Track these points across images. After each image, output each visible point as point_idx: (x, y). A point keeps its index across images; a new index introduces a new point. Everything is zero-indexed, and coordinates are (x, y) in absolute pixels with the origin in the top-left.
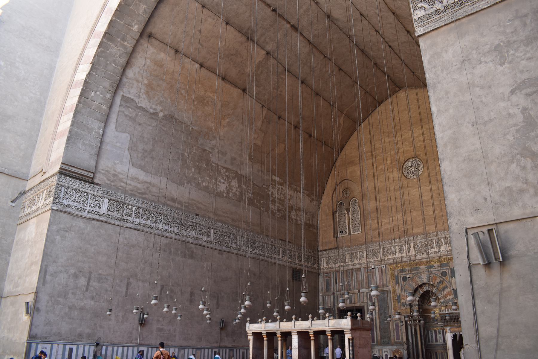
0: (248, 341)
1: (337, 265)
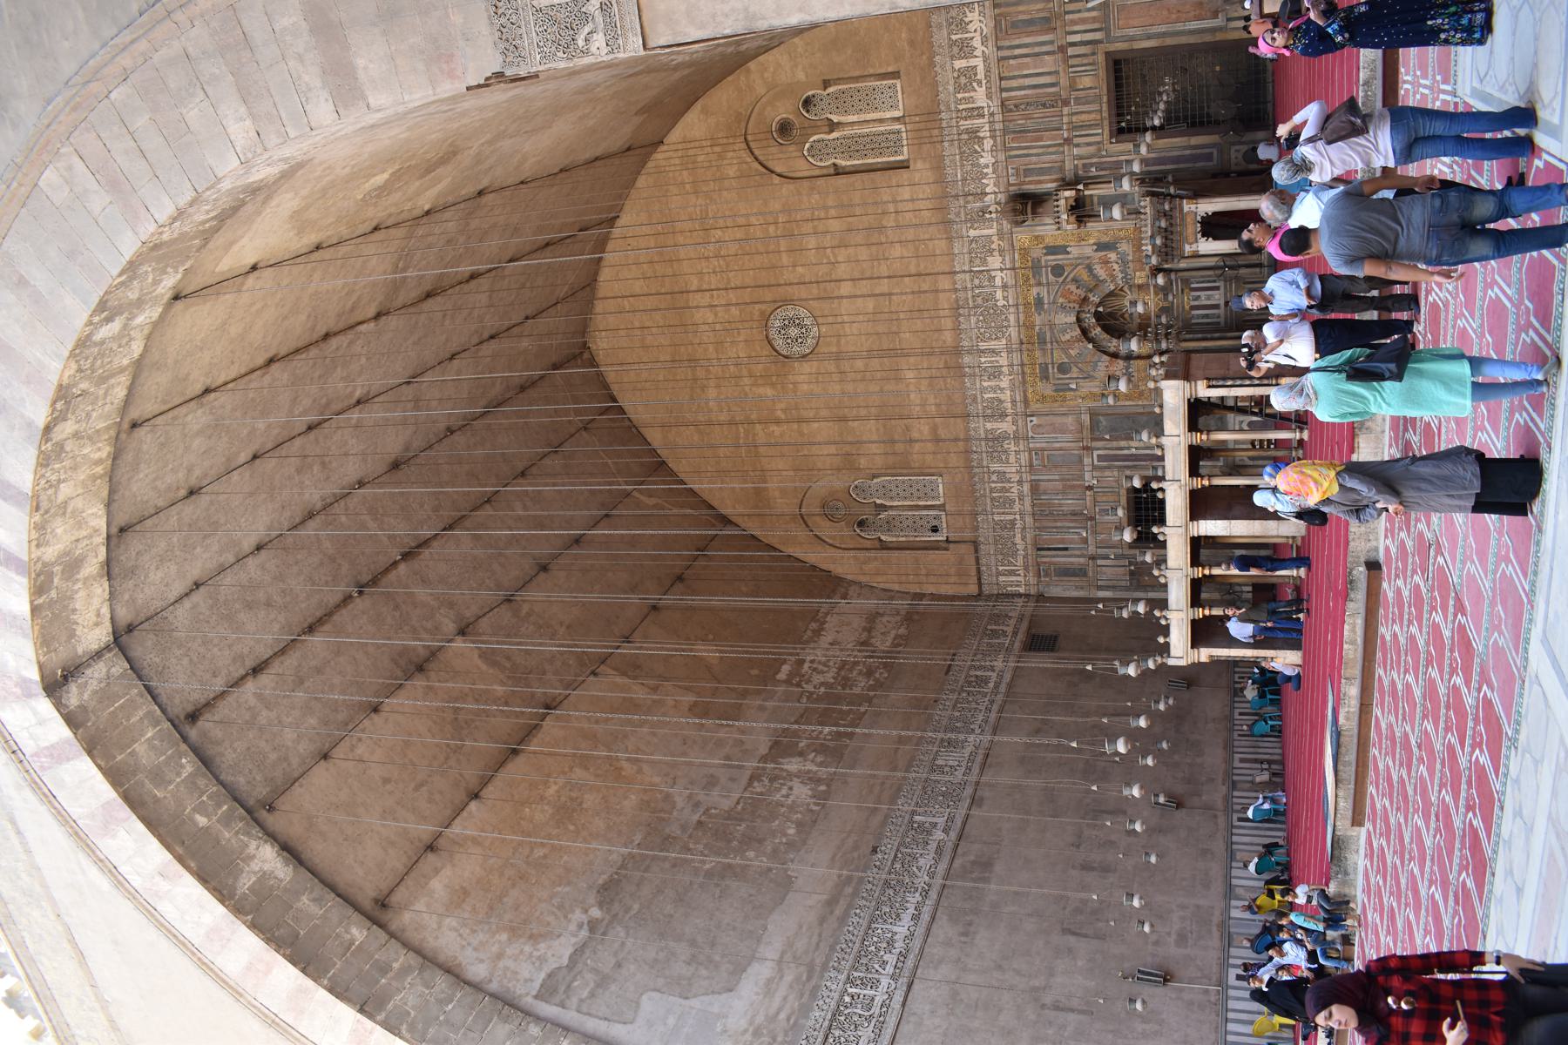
0: (1215, 662)
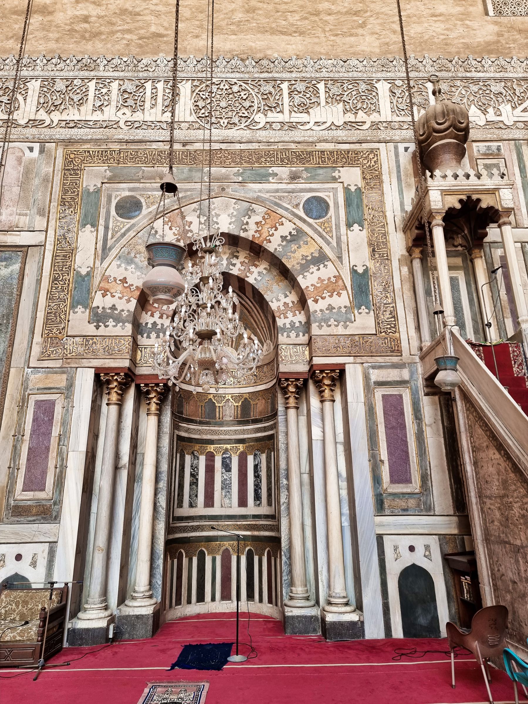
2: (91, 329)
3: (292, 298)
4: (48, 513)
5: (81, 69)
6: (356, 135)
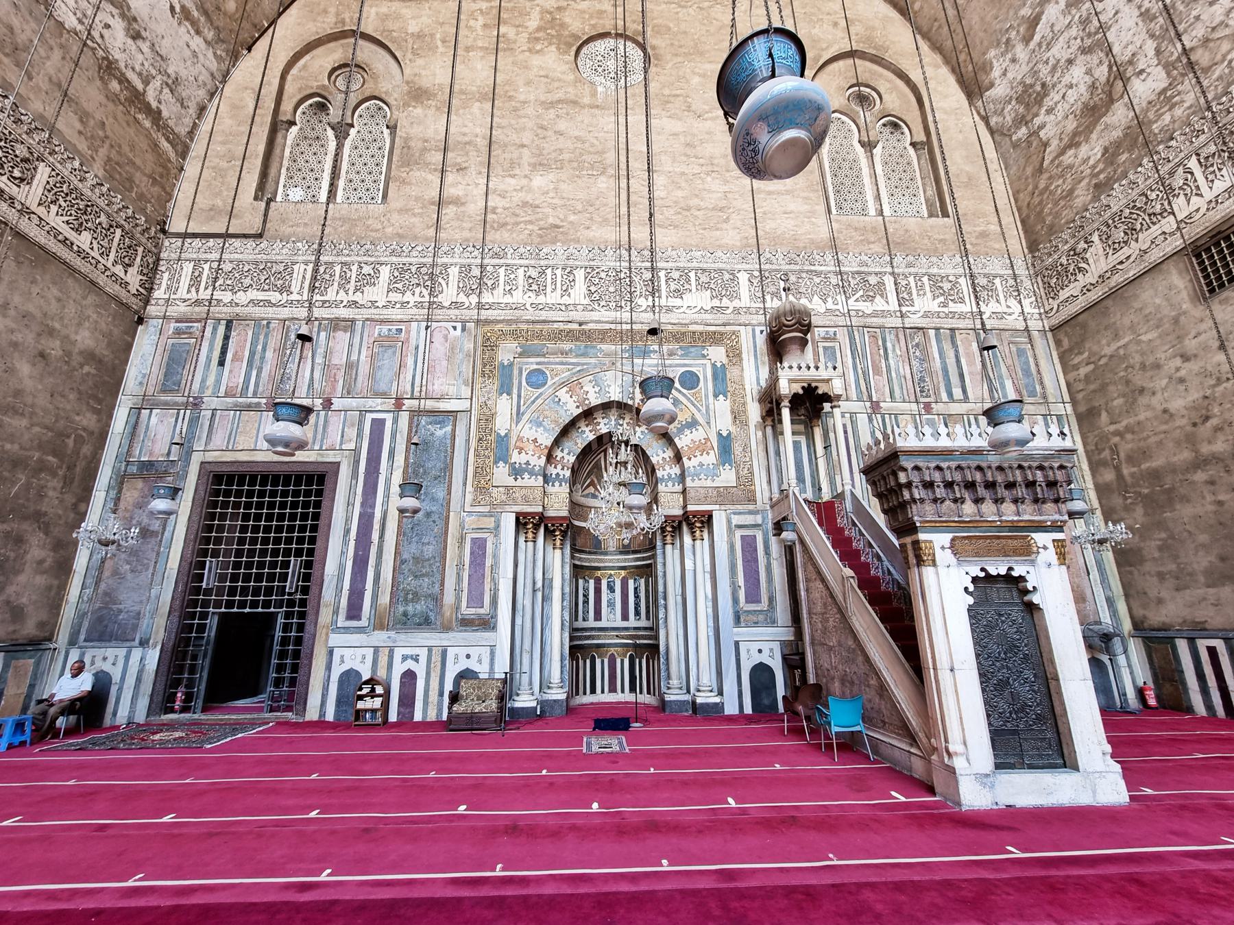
1: (242, 297)
2: (510, 481)
3: (669, 453)
4: (487, 624)
5: (492, 257)
6: (721, 318)
